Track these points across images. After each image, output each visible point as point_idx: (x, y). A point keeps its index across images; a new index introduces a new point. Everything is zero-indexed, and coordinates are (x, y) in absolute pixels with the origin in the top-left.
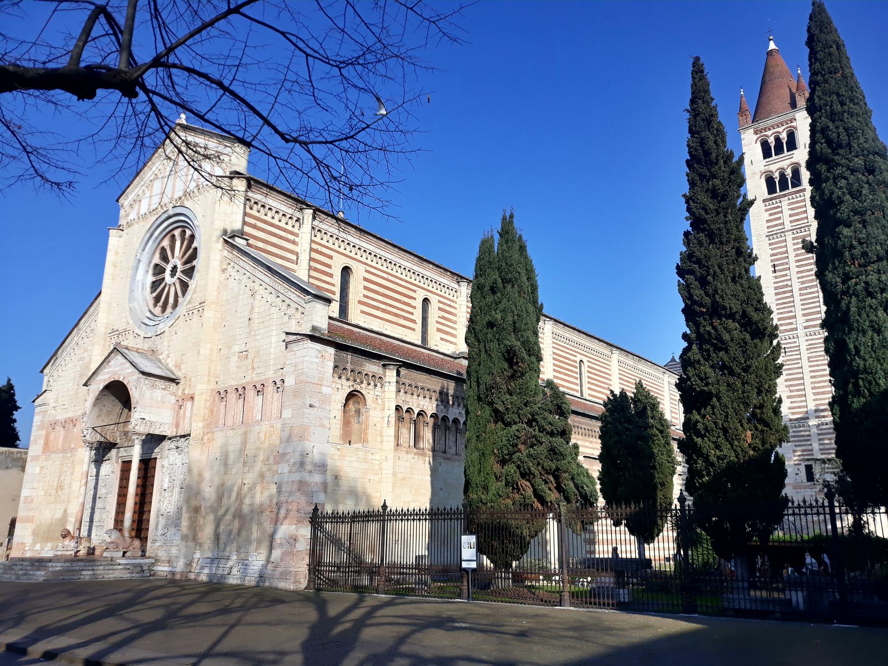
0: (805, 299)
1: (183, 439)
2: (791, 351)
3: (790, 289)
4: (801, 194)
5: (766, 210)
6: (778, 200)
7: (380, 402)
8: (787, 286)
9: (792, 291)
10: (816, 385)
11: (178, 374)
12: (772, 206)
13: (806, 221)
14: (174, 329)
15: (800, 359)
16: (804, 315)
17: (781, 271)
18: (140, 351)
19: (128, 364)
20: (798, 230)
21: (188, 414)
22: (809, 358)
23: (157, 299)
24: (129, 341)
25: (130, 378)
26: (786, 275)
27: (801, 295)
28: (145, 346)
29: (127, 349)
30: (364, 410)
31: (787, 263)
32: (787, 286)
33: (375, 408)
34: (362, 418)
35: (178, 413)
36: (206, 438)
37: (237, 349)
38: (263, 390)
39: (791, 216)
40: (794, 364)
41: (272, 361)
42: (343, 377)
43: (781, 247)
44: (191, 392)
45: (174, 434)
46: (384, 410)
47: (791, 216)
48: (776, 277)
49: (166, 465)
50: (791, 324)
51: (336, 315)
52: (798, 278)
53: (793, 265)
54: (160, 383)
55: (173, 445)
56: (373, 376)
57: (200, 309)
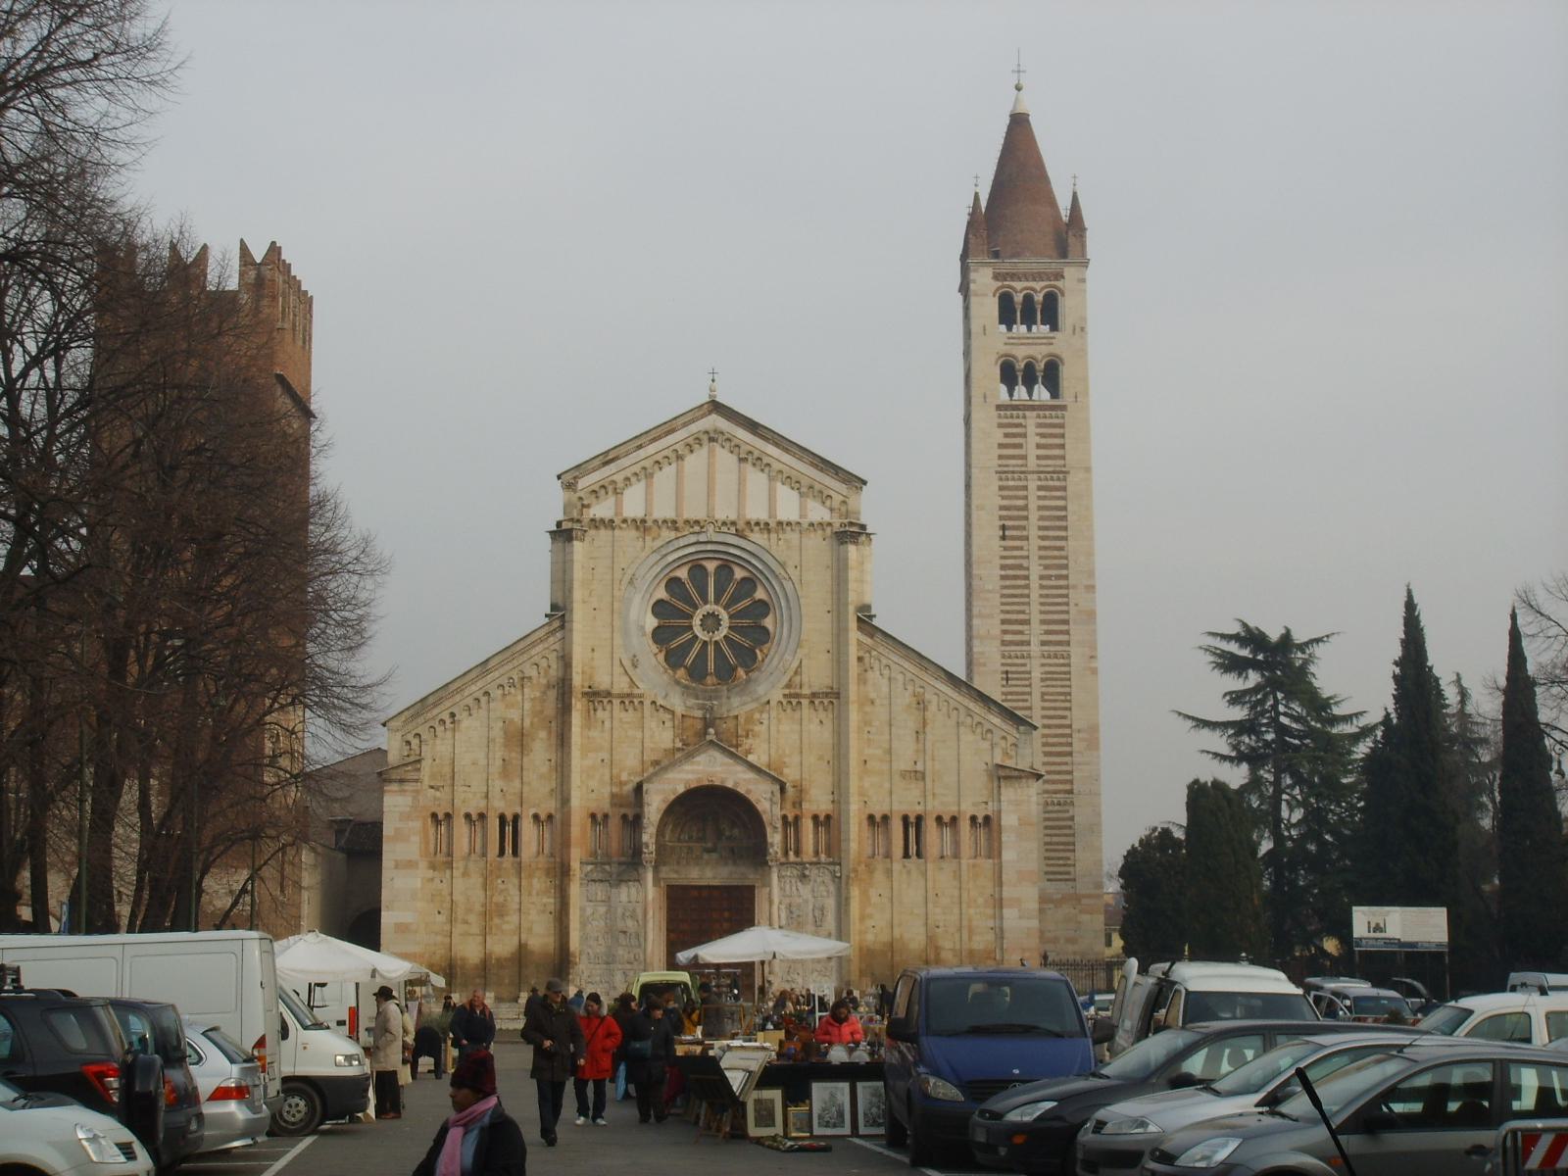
0: (1047, 596)
2: (1017, 679)
3: (1025, 573)
4: (1059, 413)
5: (1000, 426)
6: (1021, 413)
8: (1020, 567)
9: (1027, 578)
10: (1051, 740)
12: (1010, 421)
13: (1062, 462)
15: (1030, 694)
16: (1043, 622)
17: (1013, 538)
20: (1048, 476)
22: (1043, 694)
26: (1021, 548)
27: (1042, 587)
31: (1024, 528)
32: (1020, 567)
39: (1039, 446)
40: (1019, 700)
43: (1017, 498)
47: (1039, 446)
48: (1006, 549)
50: (1021, 632)
52: (1041, 558)
53: (1033, 533)
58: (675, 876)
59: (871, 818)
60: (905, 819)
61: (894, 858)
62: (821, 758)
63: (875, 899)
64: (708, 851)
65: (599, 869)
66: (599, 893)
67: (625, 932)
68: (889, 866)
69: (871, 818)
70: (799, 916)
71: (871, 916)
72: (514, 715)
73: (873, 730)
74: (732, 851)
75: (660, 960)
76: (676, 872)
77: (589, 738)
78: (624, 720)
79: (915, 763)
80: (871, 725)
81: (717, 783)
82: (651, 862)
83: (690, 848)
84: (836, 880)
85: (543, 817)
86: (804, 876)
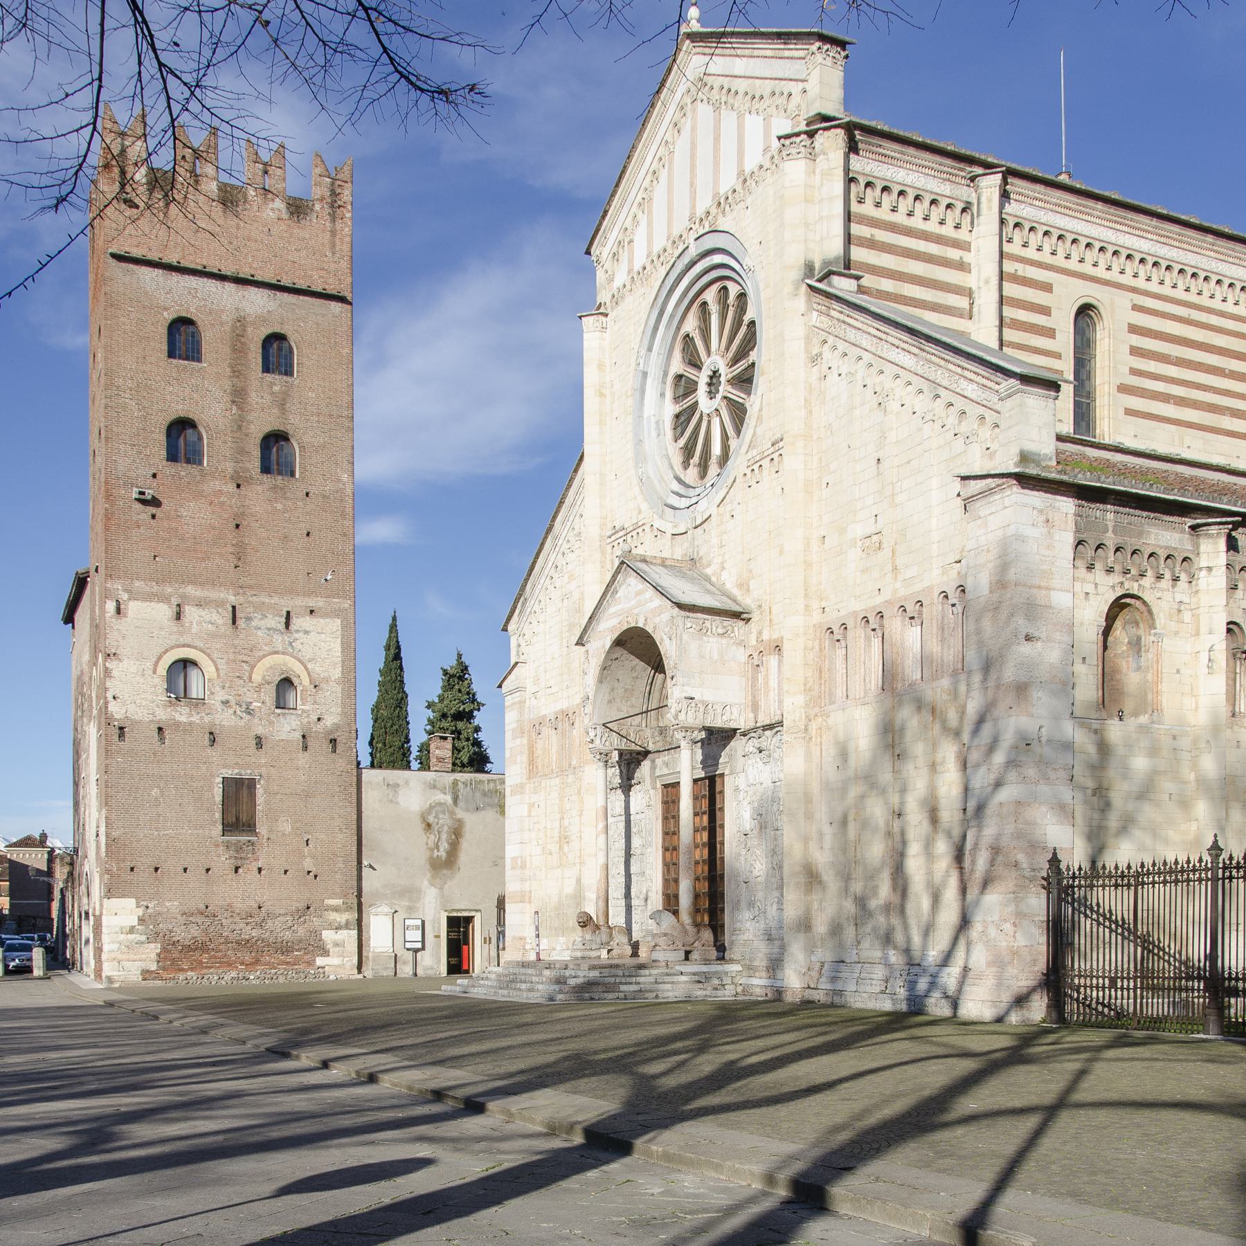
1: (768, 733)
7: (1187, 616)
11: (746, 601)
14: (727, 507)
18: (668, 563)
19: (651, 592)
21: (773, 683)
23: (688, 451)
24: (647, 546)
25: (657, 620)
28: (678, 551)
29: (644, 561)
30: (1152, 638)
33: (1176, 633)
34: (1148, 657)
35: (755, 679)
36: (813, 726)
37: (858, 530)
38: (920, 613)
41: (935, 546)
42: (1098, 566)
44: (775, 636)
45: (751, 724)
46: (1197, 634)
49: (742, 786)
51: (1067, 428)
54: (715, 623)
55: (751, 746)
56: (1168, 557)
57: (775, 456)
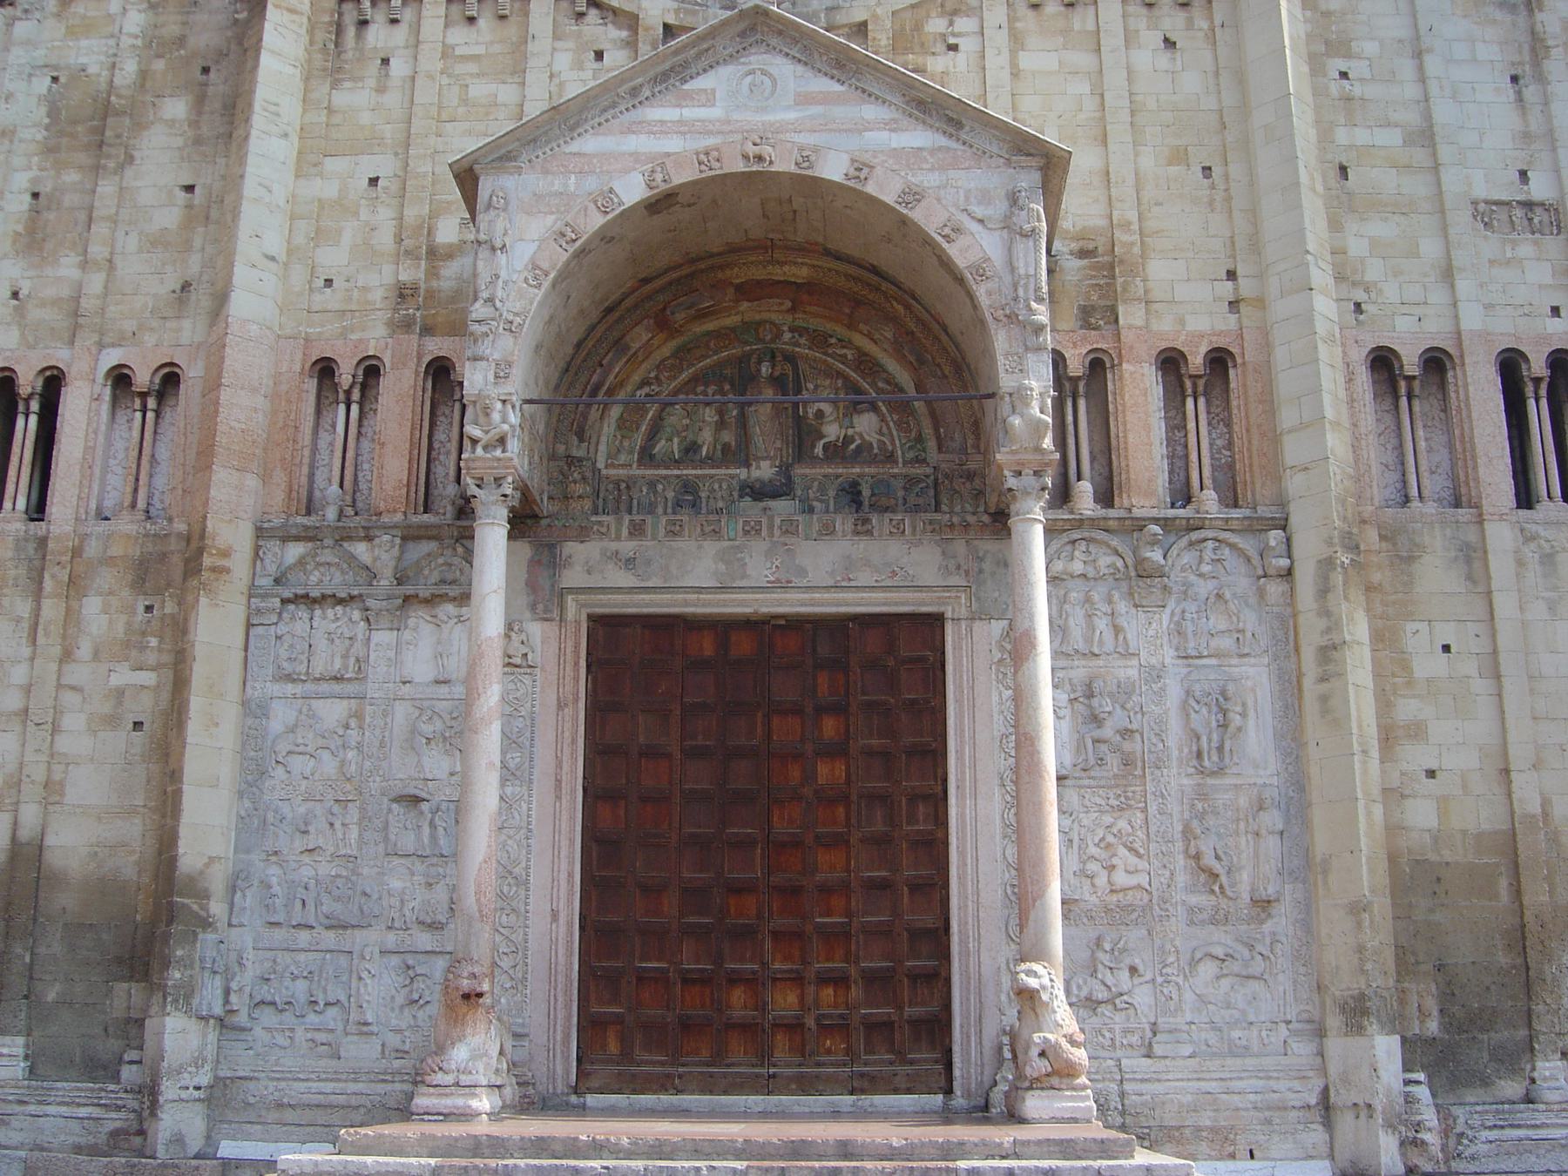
58: (625, 579)
59: (1383, 362)
60: (1510, 366)
61: (1487, 507)
62: (1179, 156)
63: (1428, 665)
64: (758, 492)
65: (327, 556)
66: (321, 644)
67: (416, 800)
68: (1472, 536)
69: (1383, 362)
70: (1126, 733)
71: (1417, 731)
72: (89, 55)
73: (1356, 68)
74: (852, 495)
75: (555, 915)
76: (630, 563)
77: (330, 110)
78: (458, 52)
79: (1523, 174)
80: (1348, 56)
81: (784, 164)
82: (498, 481)
83: (689, 487)
84: (1275, 589)
85: (143, 378)
86: (1144, 572)
